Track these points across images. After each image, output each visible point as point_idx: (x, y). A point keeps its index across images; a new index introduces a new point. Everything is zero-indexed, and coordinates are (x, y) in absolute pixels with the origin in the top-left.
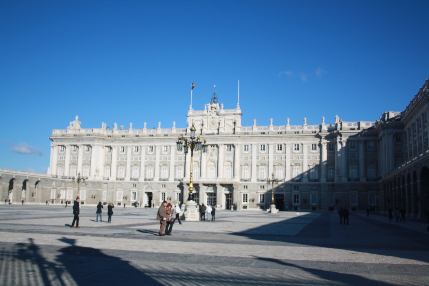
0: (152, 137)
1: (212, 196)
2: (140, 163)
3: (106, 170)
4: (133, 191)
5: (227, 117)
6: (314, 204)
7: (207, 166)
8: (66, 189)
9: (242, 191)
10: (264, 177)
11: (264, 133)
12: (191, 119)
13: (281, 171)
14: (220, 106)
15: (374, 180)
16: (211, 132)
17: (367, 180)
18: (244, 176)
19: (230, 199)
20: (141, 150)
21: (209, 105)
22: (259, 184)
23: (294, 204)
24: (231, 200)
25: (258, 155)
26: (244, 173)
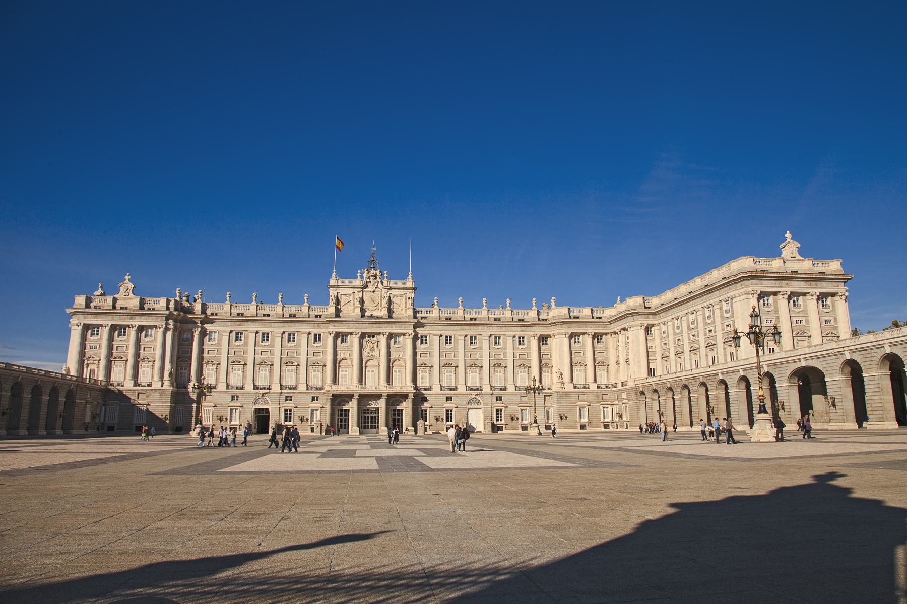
1: (368, 413)
2: (245, 359)
3: (180, 371)
5: (394, 292)
8: (104, 405)
10: (452, 384)
11: (450, 319)
12: (336, 292)
13: (477, 374)
15: (607, 387)
17: (598, 387)
18: (422, 382)
19: (397, 417)
20: (247, 338)
21: (366, 272)
22: (445, 394)
24: (398, 419)
26: (422, 378)
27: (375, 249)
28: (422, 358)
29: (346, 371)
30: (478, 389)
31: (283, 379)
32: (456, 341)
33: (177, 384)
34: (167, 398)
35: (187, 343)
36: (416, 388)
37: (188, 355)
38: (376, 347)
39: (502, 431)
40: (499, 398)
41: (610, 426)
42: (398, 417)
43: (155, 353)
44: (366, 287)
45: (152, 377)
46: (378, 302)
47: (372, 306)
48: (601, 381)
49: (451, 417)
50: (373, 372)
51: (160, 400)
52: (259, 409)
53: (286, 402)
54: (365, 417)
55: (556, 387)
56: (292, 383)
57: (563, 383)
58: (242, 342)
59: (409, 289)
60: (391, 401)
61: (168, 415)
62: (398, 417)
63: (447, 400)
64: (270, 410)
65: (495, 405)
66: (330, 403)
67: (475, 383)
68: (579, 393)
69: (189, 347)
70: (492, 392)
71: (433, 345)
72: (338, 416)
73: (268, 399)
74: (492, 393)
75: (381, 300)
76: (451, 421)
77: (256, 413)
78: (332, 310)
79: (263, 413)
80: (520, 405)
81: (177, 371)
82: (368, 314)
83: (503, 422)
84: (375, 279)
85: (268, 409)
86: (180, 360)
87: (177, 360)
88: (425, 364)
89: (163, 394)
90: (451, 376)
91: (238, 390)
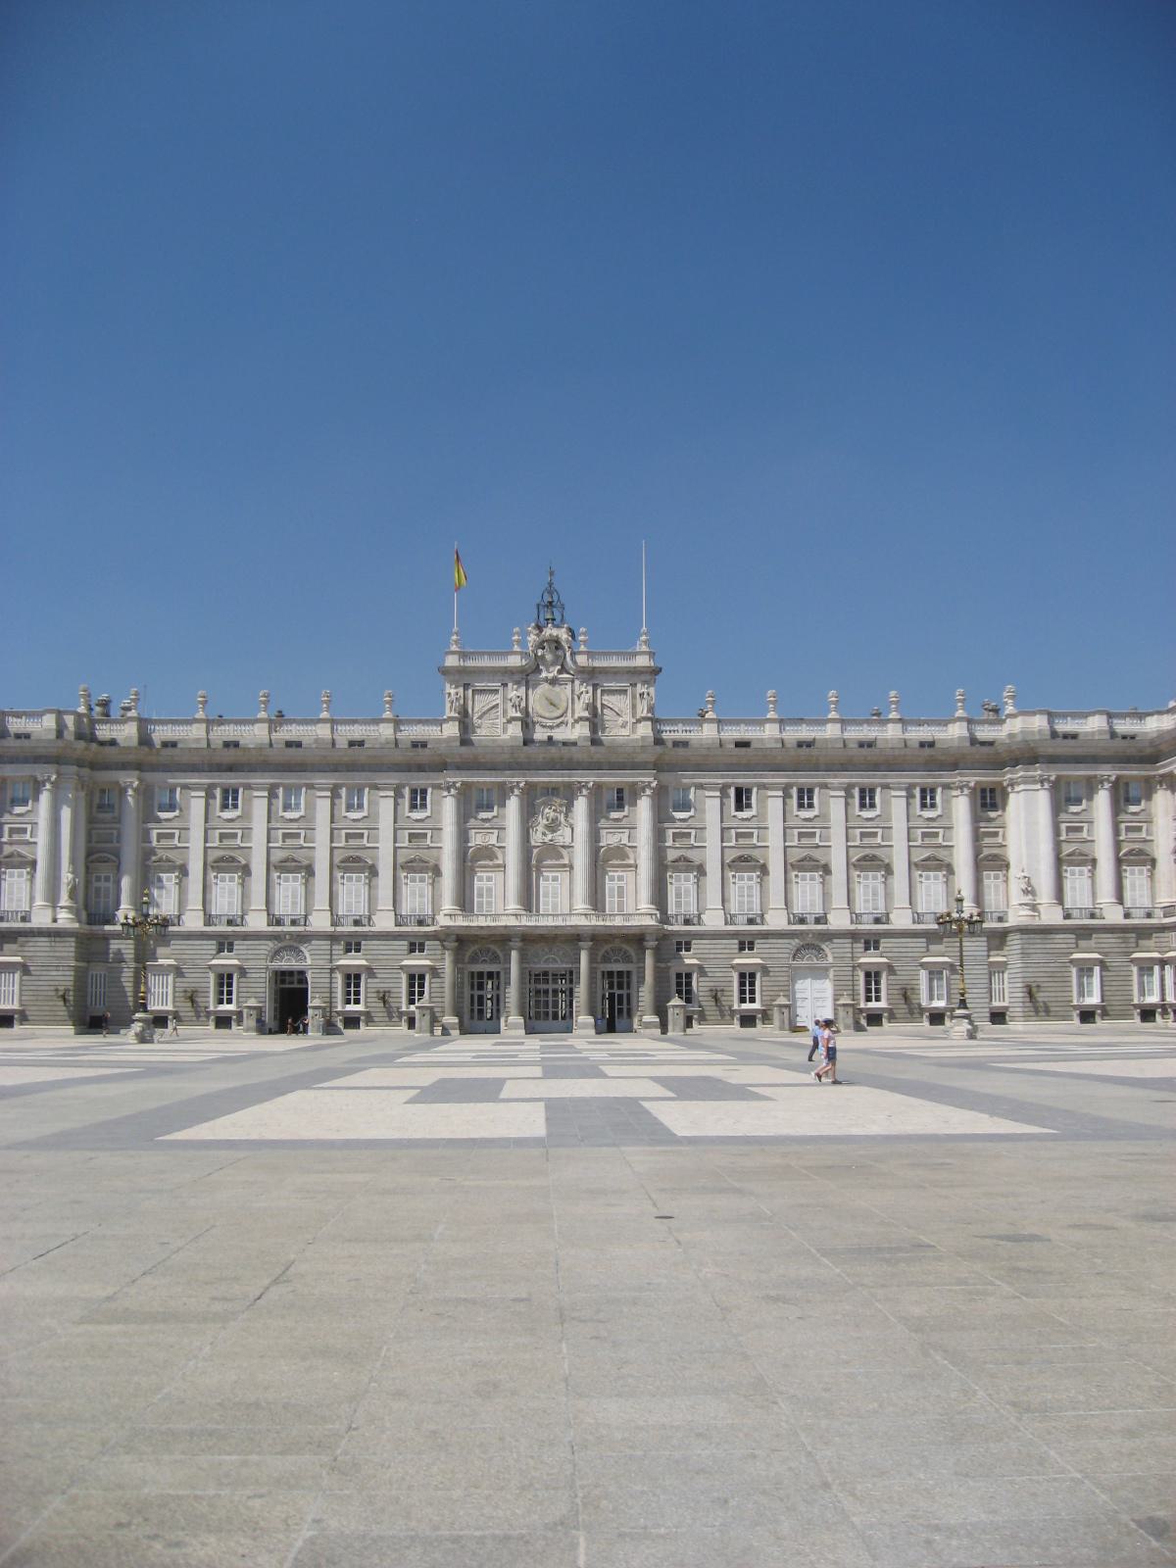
4: (221, 971)
6: (940, 1004)
12: (462, 683)
14: (572, 633)
15: (1149, 915)
17: (1127, 916)
18: (678, 904)
19: (617, 992)
23: (862, 1006)
26: (678, 895)
29: (489, 879)
30: (818, 921)
31: (338, 899)
32: (762, 802)
33: (89, 915)
34: (67, 949)
35: (108, 816)
36: (665, 919)
37: (109, 845)
38: (563, 820)
39: (881, 1025)
40: (871, 942)
41: (1158, 1017)
42: (620, 992)
43: (35, 843)
45: (32, 899)
46: (565, 704)
47: (547, 715)
48: (1133, 900)
51: (51, 954)
52: (283, 973)
53: (342, 957)
54: (538, 992)
55: (1017, 917)
56: (362, 910)
57: (1034, 907)
58: (237, 813)
59: (647, 672)
60: (600, 954)
61: (71, 988)
62: (620, 992)
63: (742, 949)
64: (309, 976)
65: (863, 960)
66: (452, 958)
67: (811, 905)
68: (1078, 932)
69: (115, 825)
70: (853, 927)
72: (472, 988)
75: (573, 699)
76: (752, 1000)
77: (276, 983)
78: (451, 730)
79: (292, 983)
80: (925, 960)
81: (88, 883)
82: (540, 734)
83: (883, 1004)
84: (557, 648)
85: (302, 973)
86: (91, 858)
87: (89, 854)
88: (687, 860)
89: (58, 939)
91: (230, 929)
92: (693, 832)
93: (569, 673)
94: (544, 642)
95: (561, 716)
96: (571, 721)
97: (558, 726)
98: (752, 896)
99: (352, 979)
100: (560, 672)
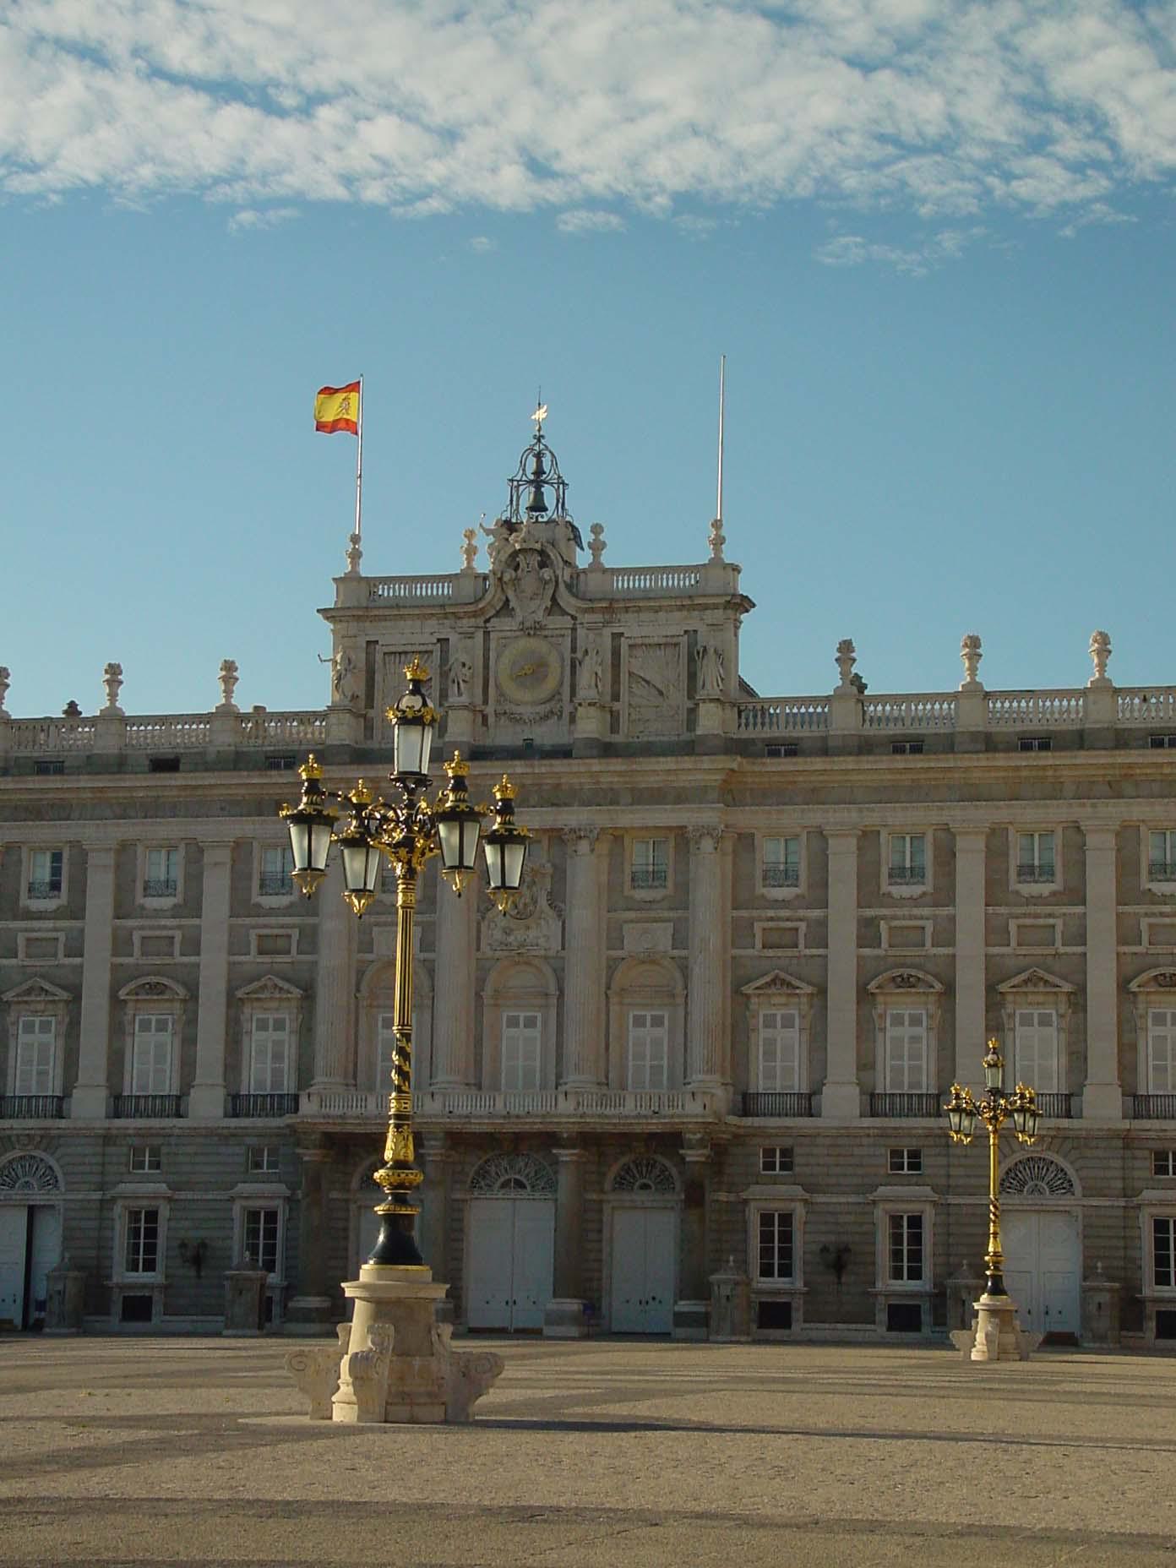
0: (53, 782)
5: (633, 628)
7: (478, 996)
9: (755, 1191)
10: (919, 1085)
13: (1051, 1031)
16: (506, 735)
18: (770, 1075)
22: (884, 1134)
25: (869, 913)
27: (541, 414)
28: (771, 953)
32: (947, 857)
38: (543, 902)
44: (506, 609)
49: (915, 1256)
50: (530, 1023)
59: (715, 607)
60: (611, 1175)
71: (826, 885)
73: (52, 1162)
74: (1127, 1141)
75: (573, 666)
84: (542, 565)
88: (789, 985)
90: (915, 1039)
92: (803, 926)
93: (564, 613)
94: (516, 553)
95: (549, 700)
96: (568, 709)
97: (546, 717)
98: (919, 1058)
99: (145, 1224)
100: (549, 612)
